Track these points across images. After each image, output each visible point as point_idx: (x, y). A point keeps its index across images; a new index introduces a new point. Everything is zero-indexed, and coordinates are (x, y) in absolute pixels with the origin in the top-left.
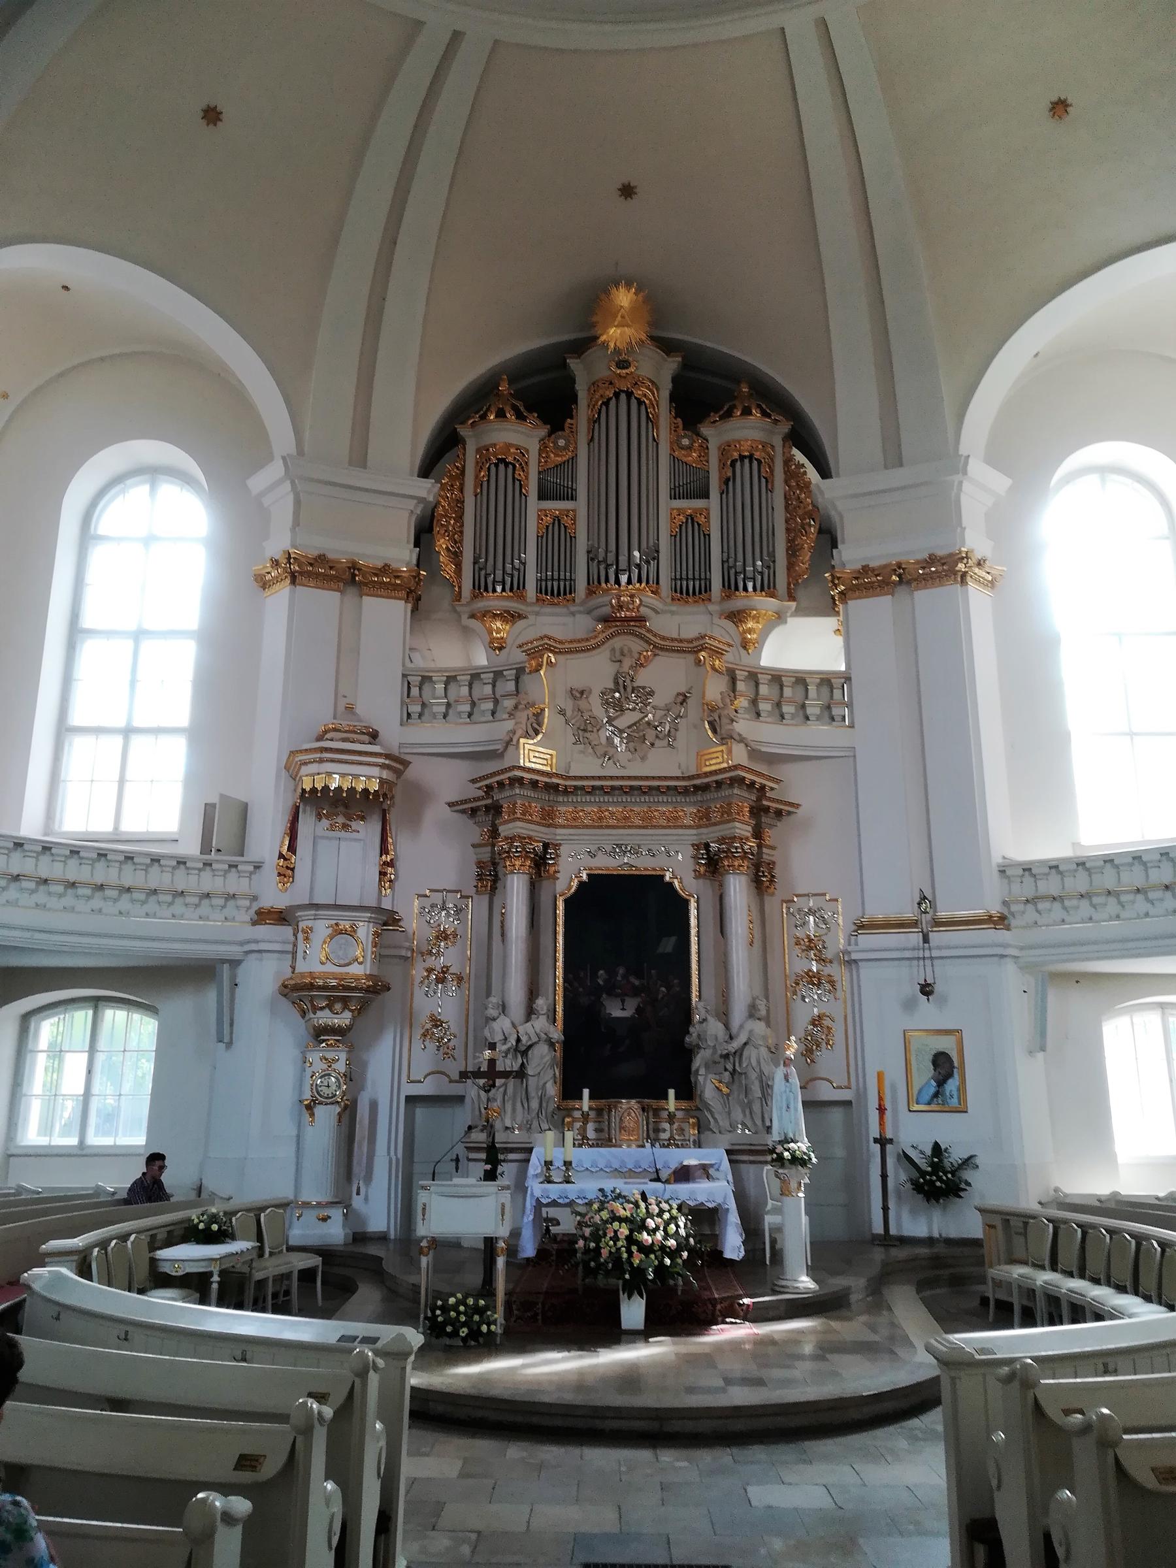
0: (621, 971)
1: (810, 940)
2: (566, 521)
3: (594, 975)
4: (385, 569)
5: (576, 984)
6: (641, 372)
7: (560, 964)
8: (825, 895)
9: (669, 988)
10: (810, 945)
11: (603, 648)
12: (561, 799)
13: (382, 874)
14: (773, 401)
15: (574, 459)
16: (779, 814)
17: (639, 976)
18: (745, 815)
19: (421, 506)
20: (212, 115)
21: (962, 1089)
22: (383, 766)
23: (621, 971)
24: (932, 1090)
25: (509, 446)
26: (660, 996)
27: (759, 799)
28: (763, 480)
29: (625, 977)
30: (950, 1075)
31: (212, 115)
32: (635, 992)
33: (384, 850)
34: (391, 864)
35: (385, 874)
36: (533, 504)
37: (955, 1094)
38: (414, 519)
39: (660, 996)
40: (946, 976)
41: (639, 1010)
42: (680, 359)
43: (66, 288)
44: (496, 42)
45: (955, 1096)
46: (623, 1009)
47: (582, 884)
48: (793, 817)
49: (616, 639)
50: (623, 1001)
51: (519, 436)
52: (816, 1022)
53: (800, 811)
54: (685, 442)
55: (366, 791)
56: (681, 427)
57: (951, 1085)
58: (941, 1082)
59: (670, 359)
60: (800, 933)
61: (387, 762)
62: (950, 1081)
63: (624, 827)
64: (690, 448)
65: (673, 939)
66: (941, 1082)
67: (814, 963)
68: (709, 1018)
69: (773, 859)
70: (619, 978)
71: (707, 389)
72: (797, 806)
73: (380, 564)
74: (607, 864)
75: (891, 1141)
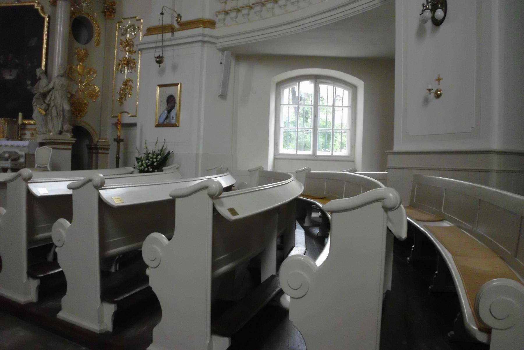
1: (127, 41)
8: (135, 17)
10: (128, 44)
21: (178, 116)
24: (165, 116)
30: (173, 107)
37: (174, 117)
40: (168, 54)
46: (11, 75)
52: (126, 83)
57: (173, 113)
58: (169, 112)
60: (123, 38)
62: (173, 111)
66: (169, 112)
68: (42, 77)
75: (122, 140)
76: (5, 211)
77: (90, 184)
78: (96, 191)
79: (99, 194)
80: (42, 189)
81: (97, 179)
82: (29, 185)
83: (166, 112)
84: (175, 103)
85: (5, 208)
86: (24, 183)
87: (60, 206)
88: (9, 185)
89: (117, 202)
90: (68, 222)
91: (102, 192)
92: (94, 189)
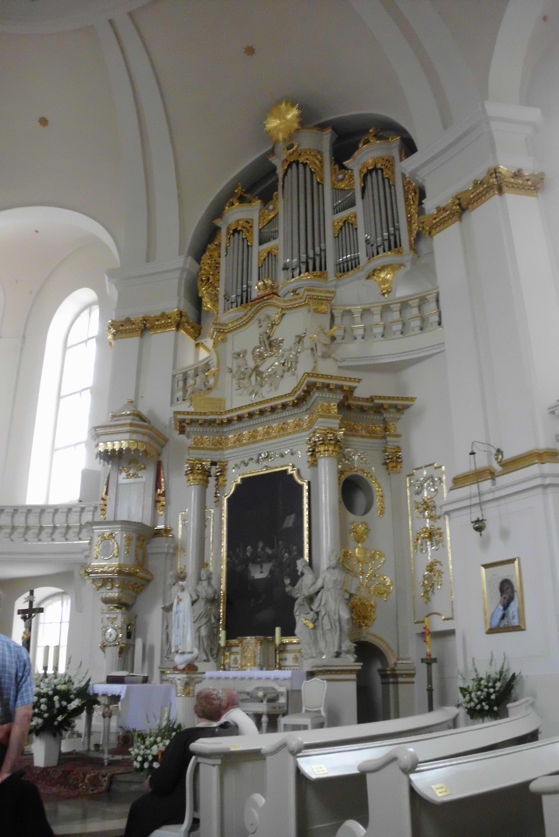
0: (261, 545)
2: (275, 252)
3: (245, 551)
4: (163, 315)
5: (234, 558)
6: (301, 147)
7: (224, 543)
8: (433, 464)
9: (290, 553)
10: (427, 506)
11: (252, 322)
12: (225, 430)
13: (157, 502)
14: (387, 129)
17: (272, 547)
18: (368, 417)
19: (185, 273)
20: (44, 122)
21: (521, 611)
22: (144, 434)
23: (261, 545)
24: (500, 614)
25: (238, 221)
26: (284, 560)
27: (346, 398)
28: (386, 181)
29: (263, 549)
30: (511, 599)
31: (44, 122)
32: (269, 558)
33: (158, 485)
34: (163, 494)
35: (158, 501)
36: (256, 249)
37: (516, 614)
38: (183, 281)
39: (284, 560)
40: (491, 515)
41: (271, 572)
43: (37, 231)
45: (516, 617)
46: (261, 572)
47: (238, 487)
48: (412, 408)
49: (261, 312)
50: (261, 566)
51: (247, 213)
52: (431, 568)
53: (416, 403)
54: (340, 177)
55: (121, 450)
56: (337, 169)
57: (513, 607)
58: (506, 606)
59: (327, 132)
60: (418, 499)
61: (132, 428)
63: (267, 439)
64: (343, 180)
65: (293, 516)
66: (506, 606)
67: (428, 521)
68: (306, 572)
70: (259, 550)
71: (347, 139)
72: (412, 399)
73: (159, 313)
74: (256, 470)
75: (435, 660)
76: (263, 800)
77: (394, 765)
78: (404, 777)
79: (410, 781)
80: (320, 766)
81: (405, 757)
82: (298, 759)
83: (501, 607)
84: (513, 591)
85: (264, 796)
86: (291, 757)
87: (348, 795)
88: (269, 759)
89: (440, 795)
90: (361, 827)
91: (413, 777)
92: (401, 772)
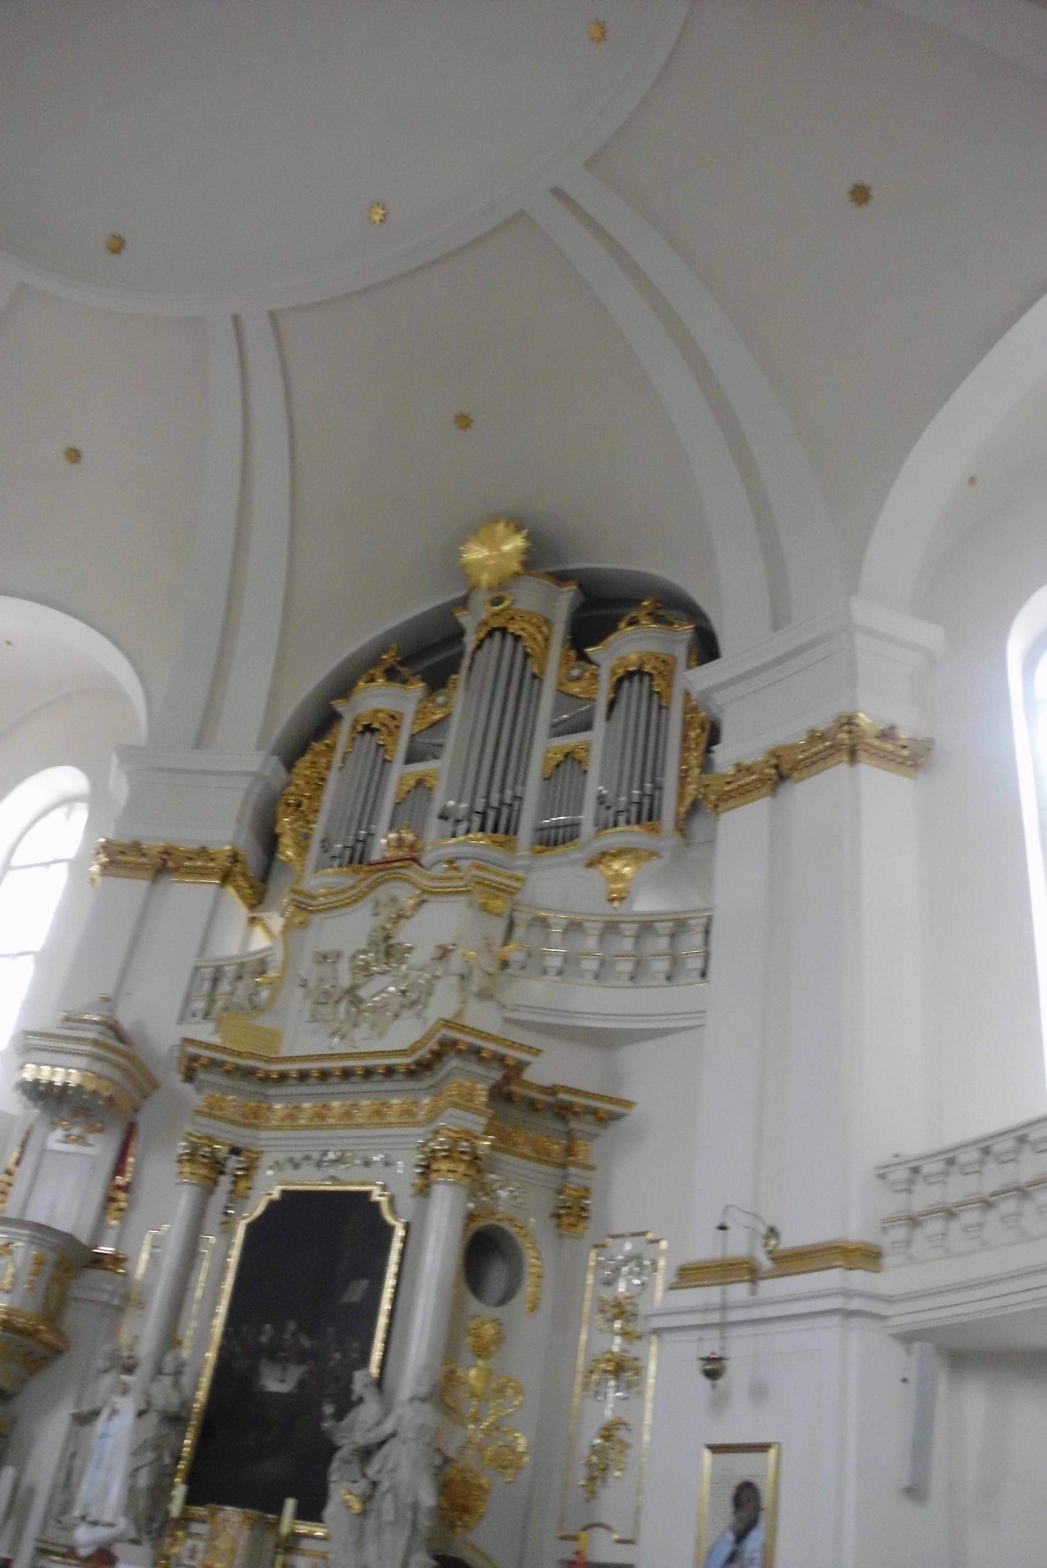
0: (292, 1326)
1: (618, 1304)
3: (260, 1332)
4: (203, 852)
6: (516, 606)
7: (222, 1309)
10: (621, 1310)
13: (111, 1199)
14: (673, 606)
15: (447, 717)
16: (603, 1119)
18: (541, 1121)
22: (117, 1066)
23: (292, 1326)
25: (377, 711)
27: (507, 1080)
29: (295, 1334)
32: (302, 1357)
33: (119, 1168)
34: (126, 1188)
40: (740, 1350)
41: (301, 1384)
42: (574, 587)
43: (9, 643)
44: (272, 315)
46: (282, 1381)
47: (272, 1205)
50: (285, 1369)
52: (608, 1432)
53: (635, 1112)
54: (575, 673)
55: (65, 1086)
56: (573, 658)
59: (565, 589)
60: (606, 1294)
64: (578, 679)
67: (618, 1340)
69: (587, 1183)
70: (287, 1336)
71: (599, 608)
72: (629, 1104)
73: (195, 846)
83: (730, 1537)
84: (758, 1508)
